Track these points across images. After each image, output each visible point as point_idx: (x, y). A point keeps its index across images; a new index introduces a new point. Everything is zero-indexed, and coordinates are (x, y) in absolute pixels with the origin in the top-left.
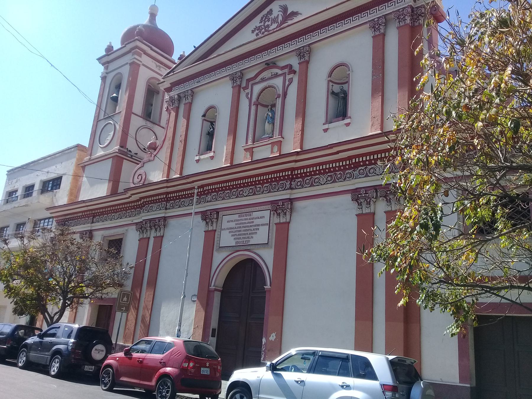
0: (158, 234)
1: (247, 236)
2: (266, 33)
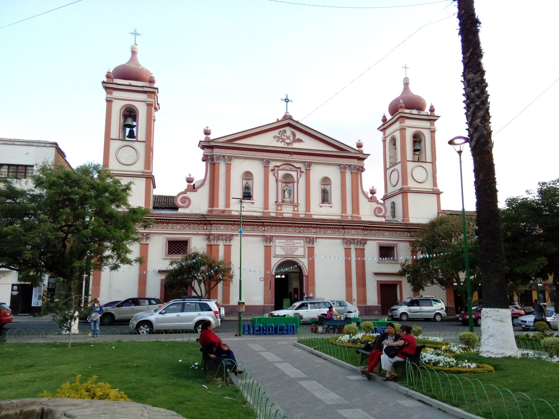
0: (227, 243)
1: (292, 251)
2: (283, 143)
